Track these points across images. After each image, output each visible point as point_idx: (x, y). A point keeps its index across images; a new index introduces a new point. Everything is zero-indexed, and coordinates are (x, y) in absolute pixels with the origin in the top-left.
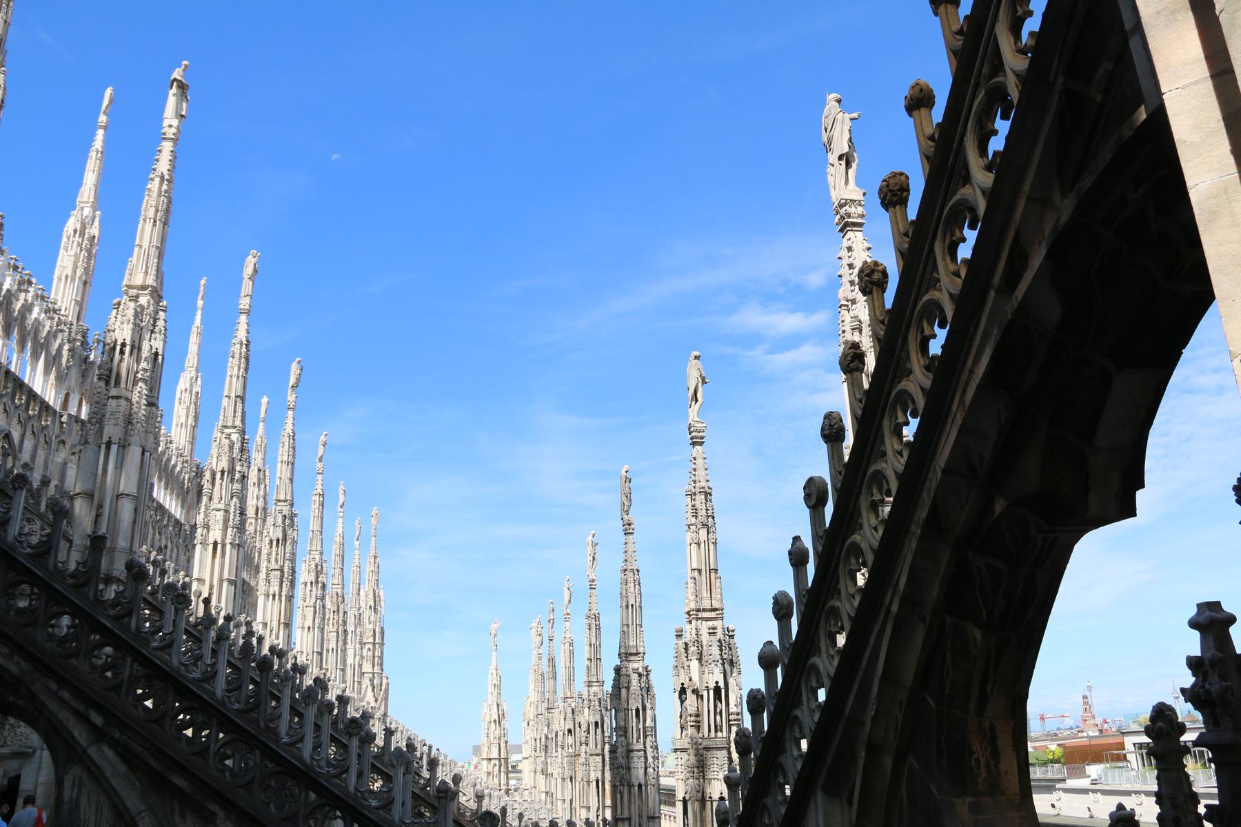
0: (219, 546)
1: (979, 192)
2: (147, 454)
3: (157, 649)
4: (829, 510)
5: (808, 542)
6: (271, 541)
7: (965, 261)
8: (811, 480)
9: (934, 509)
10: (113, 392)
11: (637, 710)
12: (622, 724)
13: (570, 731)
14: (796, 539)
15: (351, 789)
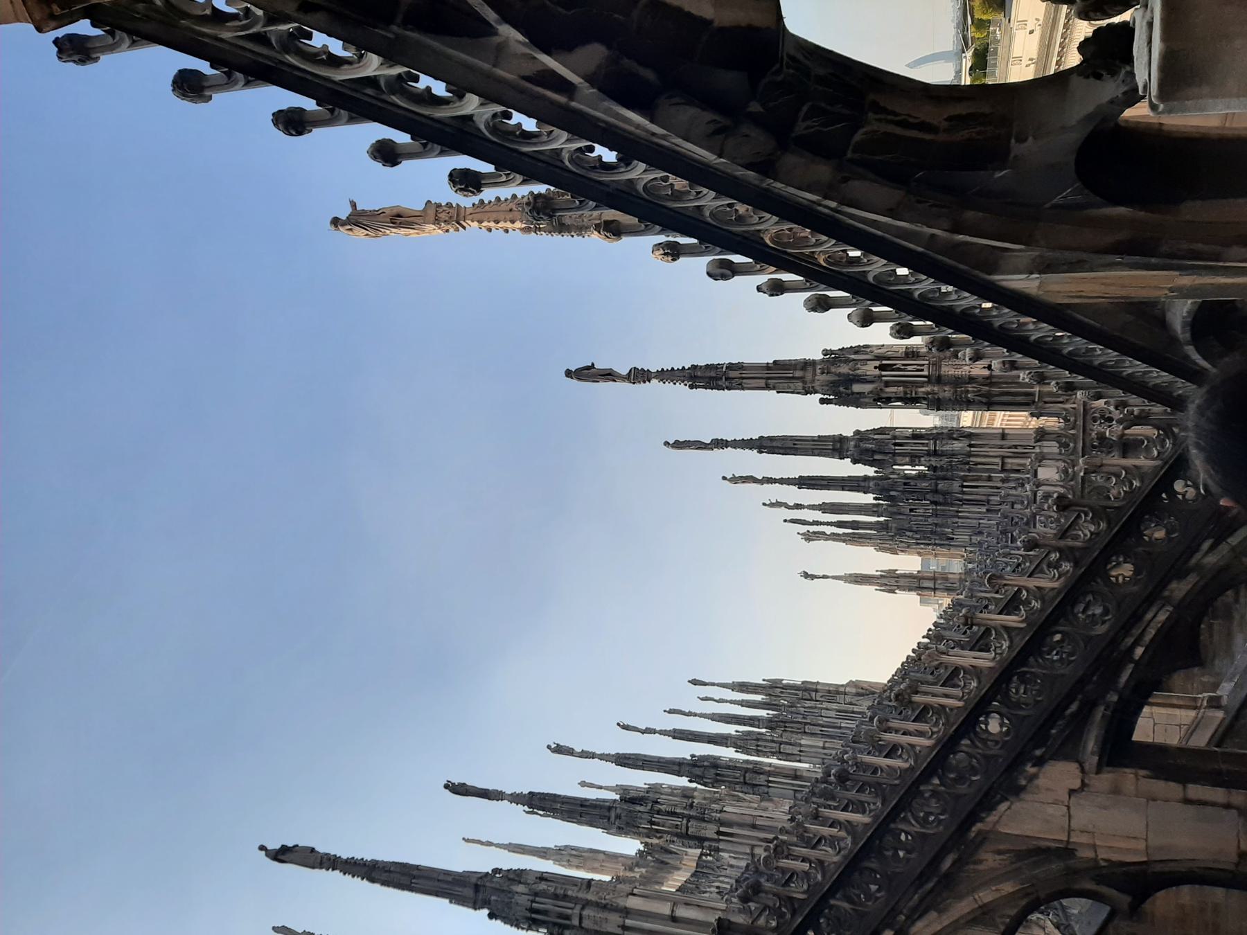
0: (722, 829)
1: (483, 110)
2: (635, 891)
3: (824, 876)
4: (737, 259)
5: (762, 279)
6: (717, 781)
7: (538, 126)
8: (709, 274)
9: (748, 167)
10: (576, 922)
11: (895, 444)
12: (907, 459)
13: (911, 510)
14: (759, 289)
15: (960, 704)
